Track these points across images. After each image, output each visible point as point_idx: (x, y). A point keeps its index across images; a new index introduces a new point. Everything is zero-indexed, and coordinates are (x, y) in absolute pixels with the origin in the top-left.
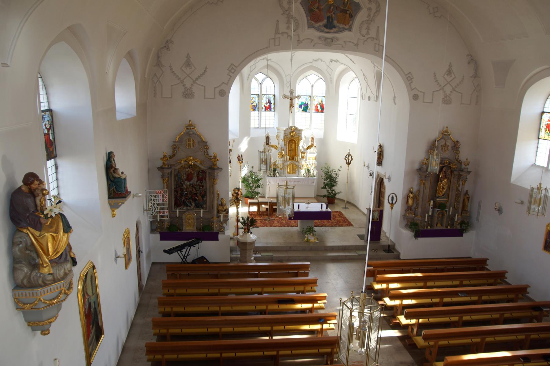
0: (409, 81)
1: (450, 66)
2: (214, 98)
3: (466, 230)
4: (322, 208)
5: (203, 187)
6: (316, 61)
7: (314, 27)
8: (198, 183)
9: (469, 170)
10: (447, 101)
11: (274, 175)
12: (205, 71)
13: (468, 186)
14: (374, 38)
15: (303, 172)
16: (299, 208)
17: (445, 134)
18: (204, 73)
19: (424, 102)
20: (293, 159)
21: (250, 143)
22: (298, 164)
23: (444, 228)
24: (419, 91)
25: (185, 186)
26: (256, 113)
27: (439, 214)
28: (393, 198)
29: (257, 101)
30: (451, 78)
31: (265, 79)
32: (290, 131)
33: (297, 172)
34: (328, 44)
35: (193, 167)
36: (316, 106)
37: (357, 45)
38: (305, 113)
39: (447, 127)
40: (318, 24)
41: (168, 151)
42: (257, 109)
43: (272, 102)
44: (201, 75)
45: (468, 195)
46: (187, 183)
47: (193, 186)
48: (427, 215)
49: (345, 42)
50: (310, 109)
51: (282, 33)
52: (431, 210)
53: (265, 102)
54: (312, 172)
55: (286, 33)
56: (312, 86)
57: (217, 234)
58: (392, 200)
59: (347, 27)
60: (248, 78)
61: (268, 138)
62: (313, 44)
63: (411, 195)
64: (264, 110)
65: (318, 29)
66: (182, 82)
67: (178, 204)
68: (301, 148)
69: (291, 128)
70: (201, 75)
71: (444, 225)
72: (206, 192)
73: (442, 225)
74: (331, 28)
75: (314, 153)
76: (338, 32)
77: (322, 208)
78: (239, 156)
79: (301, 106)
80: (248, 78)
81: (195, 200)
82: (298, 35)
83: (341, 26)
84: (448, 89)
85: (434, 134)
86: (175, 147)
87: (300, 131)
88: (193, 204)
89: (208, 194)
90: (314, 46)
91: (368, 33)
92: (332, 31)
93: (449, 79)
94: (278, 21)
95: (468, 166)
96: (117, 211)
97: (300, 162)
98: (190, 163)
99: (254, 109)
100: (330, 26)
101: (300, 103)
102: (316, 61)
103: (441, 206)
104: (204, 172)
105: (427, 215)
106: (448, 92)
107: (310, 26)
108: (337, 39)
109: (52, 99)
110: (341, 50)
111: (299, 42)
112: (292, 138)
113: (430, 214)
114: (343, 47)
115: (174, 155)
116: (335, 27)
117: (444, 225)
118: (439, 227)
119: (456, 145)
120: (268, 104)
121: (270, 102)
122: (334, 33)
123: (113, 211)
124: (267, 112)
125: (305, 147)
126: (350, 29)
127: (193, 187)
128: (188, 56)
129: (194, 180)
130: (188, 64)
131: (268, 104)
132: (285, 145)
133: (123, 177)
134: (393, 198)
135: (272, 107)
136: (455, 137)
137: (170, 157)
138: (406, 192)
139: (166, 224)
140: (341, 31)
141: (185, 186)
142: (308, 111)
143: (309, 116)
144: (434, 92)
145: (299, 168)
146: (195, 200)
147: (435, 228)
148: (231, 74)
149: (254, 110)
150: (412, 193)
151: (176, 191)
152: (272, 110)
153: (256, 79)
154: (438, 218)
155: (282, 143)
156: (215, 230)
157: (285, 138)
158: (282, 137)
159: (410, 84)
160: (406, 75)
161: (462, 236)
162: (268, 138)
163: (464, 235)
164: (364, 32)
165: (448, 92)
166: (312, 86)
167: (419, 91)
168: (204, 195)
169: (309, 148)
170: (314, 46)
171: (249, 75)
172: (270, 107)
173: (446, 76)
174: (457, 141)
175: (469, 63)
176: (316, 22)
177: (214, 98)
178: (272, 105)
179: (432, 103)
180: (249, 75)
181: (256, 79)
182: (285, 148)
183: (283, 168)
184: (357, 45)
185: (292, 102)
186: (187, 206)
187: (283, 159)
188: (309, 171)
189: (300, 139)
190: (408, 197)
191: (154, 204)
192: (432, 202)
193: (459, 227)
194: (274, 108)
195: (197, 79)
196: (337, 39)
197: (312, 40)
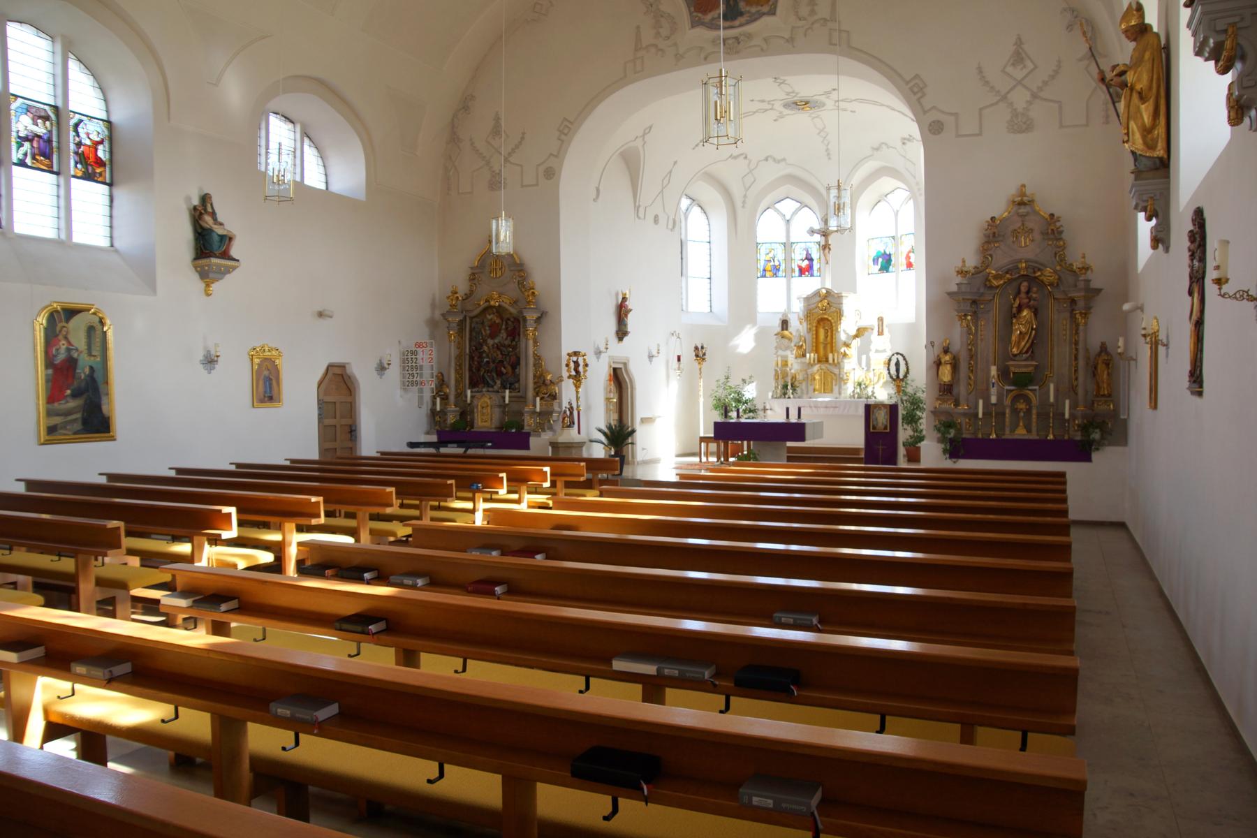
0: (915, 94)
1: (1019, 42)
2: (537, 185)
3: (1099, 445)
5: (515, 348)
6: (877, 149)
7: (703, 24)
8: (507, 342)
9: (1094, 285)
10: (1021, 125)
12: (523, 138)
13: (1097, 332)
14: (825, 20)
15: (849, 388)
17: (1022, 202)
18: (520, 143)
19: (958, 136)
20: (827, 361)
21: (759, 337)
22: (836, 371)
23: (1034, 436)
24: (943, 112)
25: (485, 348)
26: (780, 282)
27: (1015, 399)
28: (897, 364)
29: (780, 255)
30: (1025, 71)
31: (799, 209)
32: (818, 299)
33: (836, 389)
34: (734, 48)
35: (499, 310)
36: (908, 257)
37: (791, 40)
38: (885, 275)
39: (1024, 186)
40: (709, 16)
41: (463, 288)
42: (780, 273)
44: (517, 147)
45: (1108, 354)
46: (490, 342)
47: (498, 347)
48: (981, 402)
49: (766, 40)
51: (648, 46)
52: (994, 391)
55: (655, 46)
56: (896, 214)
57: (528, 435)
58: (898, 370)
59: (765, 9)
60: (744, 202)
61: (785, 324)
62: (702, 56)
63: (947, 358)
65: (713, 26)
66: (488, 163)
67: (473, 384)
70: (517, 147)
71: (1034, 429)
72: (518, 359)
73: (1029, 431)
74: (734, 18)
76: (748, 23)
78: (696, 348)
79: (875, 261)
80: (744, 202)
81: (500, 374)
82: (675, 44)
83: (753, 10)
84: (1020, 98)
85: (998, 207)
86: (473, 277)
88: (499, 382)
89: (523, 362)
90: (706, 59)
91: (813, 12)
92: (737, 23)
93: (1018, 73)
94: (638, 27)
95: (1089, 275)
96: (214, 287)
98: (492, 303)
99: (775, 271)
100: (733, 14)
101: (873, 254)
102: (877, 149)
103: (1022, 381)
104: (517, 320)
105: (981, 402)
106: (1020, 104)
107: (695, 24)
108: (749, 36)
109: (113, 108)
110: (759, 56)
111: (678, 57)
112: (823, 315)
113: (994, 400)
114: (766, 48)
115: (472, 292)
116: (741, 14)
117: (1034, 429)
118: (1021, 433)
119: (1053, 230)
120: (806, 262)
122: (741, 25)
123: (208, 285)
125: (853, 332)
126: (772, 12)
127: (498, 348)
128: (497, 119)
129: (503, 334)
130: (496, 131)
131: (806, 262)
132: (809, 330)
133: (220, 231)
134: (897, 364)
135: (816, 266)
136: (1046, 206)
137: (467, 297)
138: (937, 350)
139: (451, 419)
140: (754, 18)
141: (485, 348)
144: (981, 109)
146: (500, 374)
147: (1008, 435)
148: (563, 137)
149: (775, 275)
150: (946, 351)
151: (471, 358)
152: (815, 273)
153: (777, 211)
154: (1015, 411)
156: (526, 429)
159: (919, 100)
160: (907, 83)
161: (1089, 459)
162: (785, 324)
163: (1095, 456)
164: (804, 11)
165: (1020, 104)
166: (896, 214)
167: (943, 112)
168: (516, 364)
170: (706, 59)
171: (745, 196)
173: (1009, 69)
174: (1052, 215)
175: (1070, 27)
176: (705, 12)
177: (537, 185)
179: (980, 134)
180: (745, 196)
181: (777, 211)
182: (809, 338)
183: (806, 379)
184: (791, 40)
185: (827, 241)
186: (488, 385)
187: (803, 360)
189: (839, 314)
190: (938, 364)
191: (412, 367)
192: (994, 371)
193: (1078, 437)
195: (510, 154)
196: (749, 36)
197: (701, 48)
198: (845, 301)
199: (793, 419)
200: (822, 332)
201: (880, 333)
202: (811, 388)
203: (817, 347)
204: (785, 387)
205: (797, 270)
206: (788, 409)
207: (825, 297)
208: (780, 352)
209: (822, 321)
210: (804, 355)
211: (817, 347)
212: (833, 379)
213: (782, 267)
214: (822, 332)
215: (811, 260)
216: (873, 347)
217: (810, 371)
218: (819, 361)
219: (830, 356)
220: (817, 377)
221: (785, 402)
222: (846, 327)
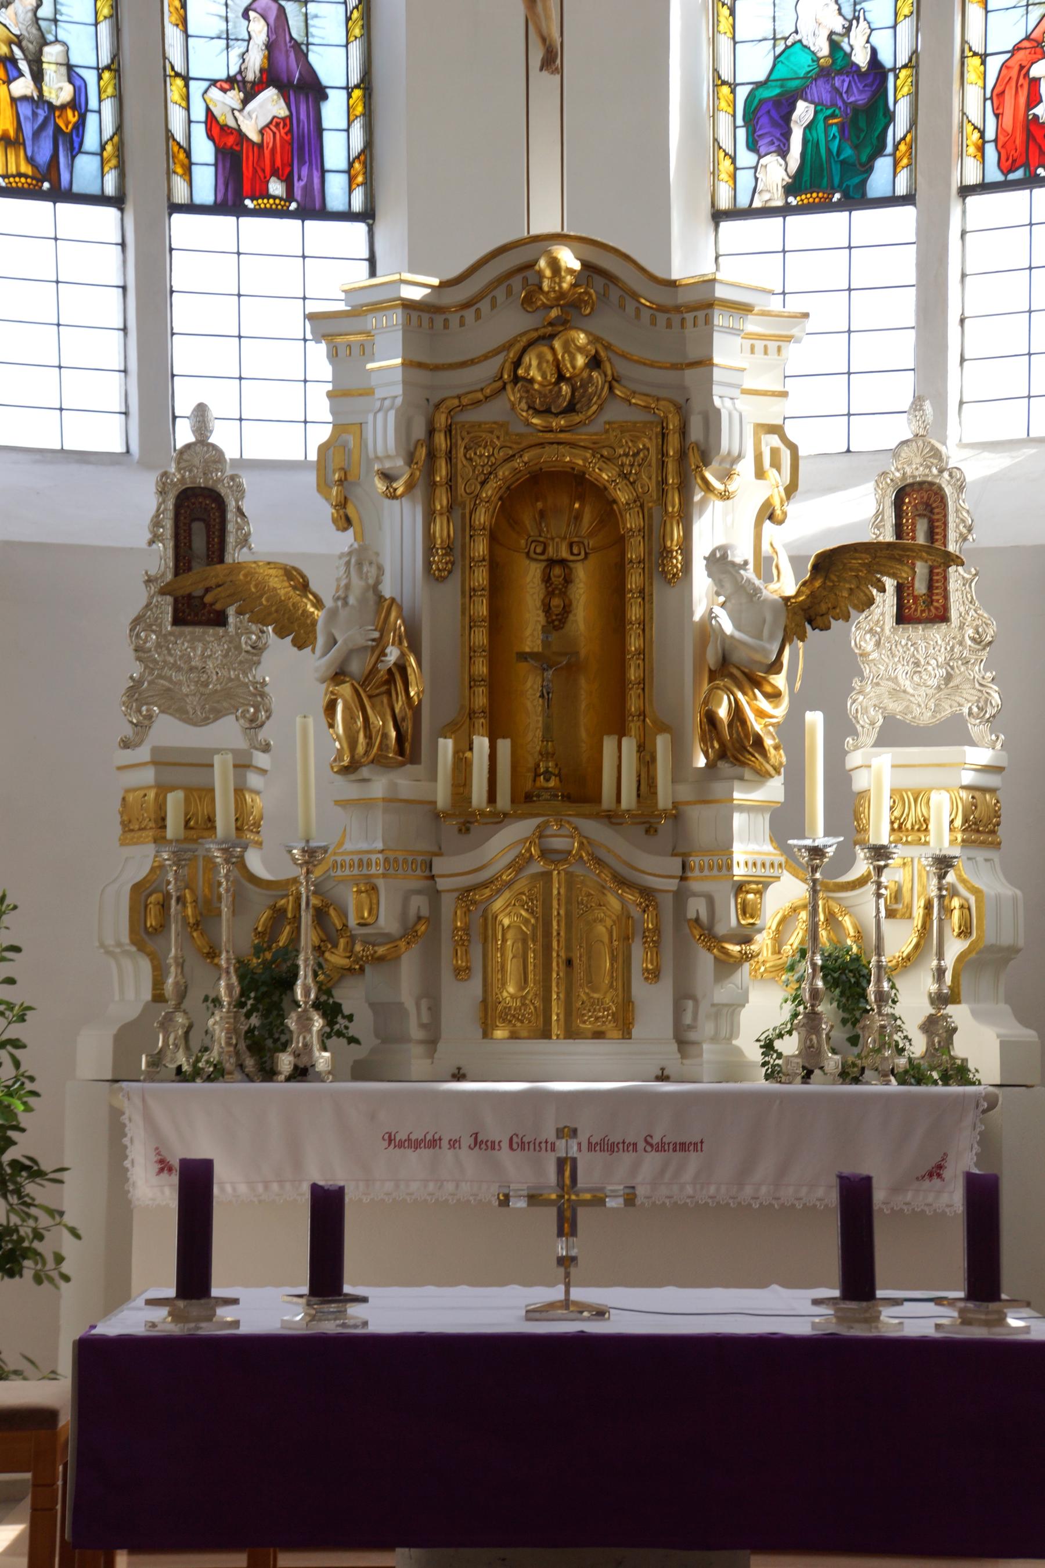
4: (858, 1281)
11: (261, 1051)
16: (326, 1278)
22: (656, 869)
32: (510, 322)
33: (653, 1002)
42: (86, 171)
43: (333, 63)
50: (910, 155)
53: (210, 60)
54: (912, 1002)
64: (205, 185)
68: (703, 593)
69: (512, 271)
75: (952, 732)
77: (858, 1281)
79: (766, 119)
87: (692, 310)
97: (698, 816)
101: (754, 65)
120: (269, 105)
121: (288, 73)
124: (263, 233)
131: (269, 105)
132: (441, 561)
142: (882, 177)
143: (905, 265)
145: (685, 931)
155: (400, 531)
157: (440, 445)
158: (383, 438)
162: (200, 510)
169: (837, 578)
172: (298, 144)
178: (334, 111)
182: (441, 615)
187: (404, 782)
188: (847, 981)
194: (365, 165)
198: (727, 350)
199: (917, 1311)
200: (530, 578)
201: (924, 608)
202: (460, 999)
203: (498, 685)
204: (266, 988)
205: (203, 150)
206: (856, 1200)
207: (571, 308)
208: (169, 732)
209: (542, 486)
210: (408, 749)
211: (498, 685)
212: (632, 924)
213: (100, 125)
214: (530, 578)
215: (306, 90)
216: (866, 706)
217: (454, 868)
218: (526, 799)
219: (618, 761)
220: (508, 915)
221: (208, 1121)
222: (746, 531)
